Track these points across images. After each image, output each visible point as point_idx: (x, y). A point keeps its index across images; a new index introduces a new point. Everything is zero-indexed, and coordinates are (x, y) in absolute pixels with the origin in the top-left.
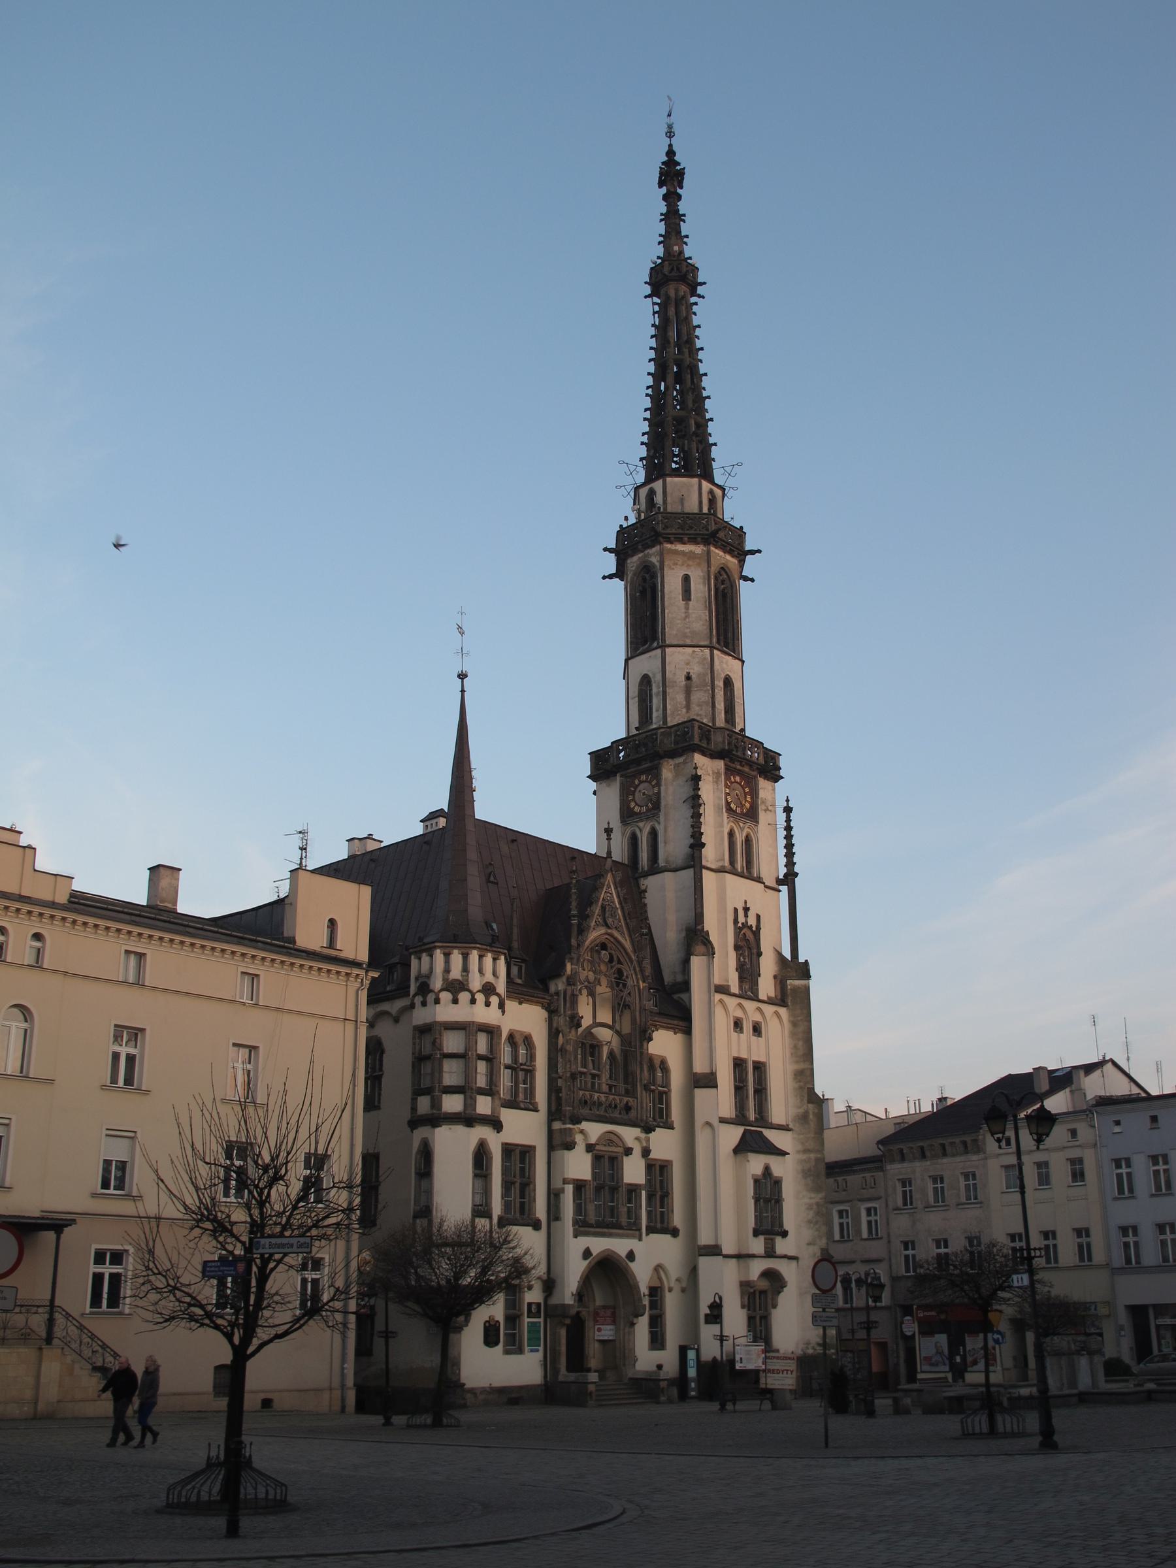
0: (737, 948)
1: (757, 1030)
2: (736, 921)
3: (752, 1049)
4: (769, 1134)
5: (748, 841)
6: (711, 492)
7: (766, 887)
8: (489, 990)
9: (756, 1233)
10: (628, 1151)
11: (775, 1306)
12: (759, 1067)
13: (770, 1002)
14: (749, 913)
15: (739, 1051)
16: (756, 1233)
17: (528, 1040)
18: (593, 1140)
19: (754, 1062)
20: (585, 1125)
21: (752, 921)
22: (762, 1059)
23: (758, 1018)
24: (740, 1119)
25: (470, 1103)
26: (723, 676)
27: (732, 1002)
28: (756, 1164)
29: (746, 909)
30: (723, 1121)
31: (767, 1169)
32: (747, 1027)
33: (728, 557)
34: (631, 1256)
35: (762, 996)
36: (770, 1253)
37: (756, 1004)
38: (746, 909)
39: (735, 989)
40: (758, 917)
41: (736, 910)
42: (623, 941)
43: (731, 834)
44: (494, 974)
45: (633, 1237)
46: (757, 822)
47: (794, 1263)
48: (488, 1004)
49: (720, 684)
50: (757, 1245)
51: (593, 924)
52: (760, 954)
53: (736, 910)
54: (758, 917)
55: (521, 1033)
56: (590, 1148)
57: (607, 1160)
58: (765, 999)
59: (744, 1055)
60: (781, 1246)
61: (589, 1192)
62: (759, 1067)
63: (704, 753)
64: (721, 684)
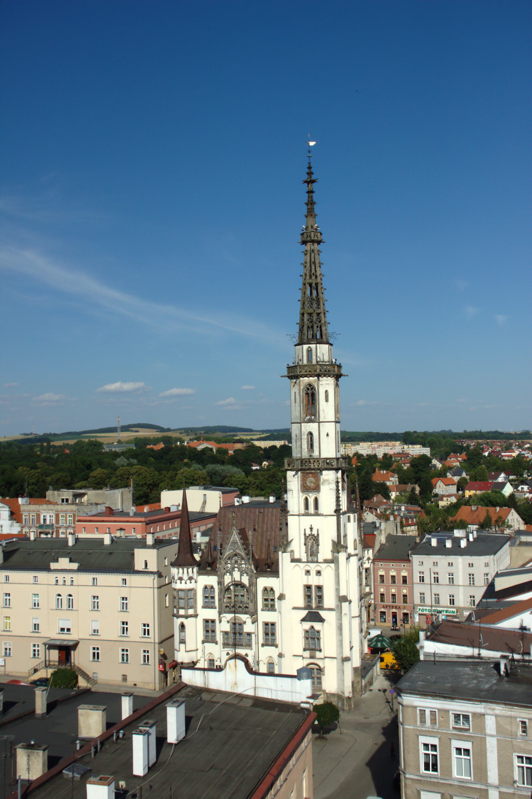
0: (305, 544)
1: (319, 573)
2: (305, 534)
3: (314, 581)
4: (323, 613)
5: (316, 500)
6: (309, 347)
7: (326, 515)
8: (181, 579)
9: (305, 650)
10: (245, 623)
11: (324, 675)
12: (319, 588)
13: (326, 561)
14: (313, 530)
15: (308, 582)
16: (305, 650)
17: (212, 587)
18: (228, 619)
19: (315, 586)
20: (224, 615)
21: (315, 532)
22: (321, 584)
23: (318, 568)
24: (308, 607)
25: (178, 611)
26: (307, 433)
27: (301, 565)
28: (307, 625)
29: (311, 529)
30: (295, 608)
31: (312, 627)
32: (313, 573)
33: (311, 378)
34: (247, 655)
35: (319, 561)
36: (312, 657)
37: (316, 564)
38: (311, 529)
39: (304, 559)
40: (318, 530)
41: (305, 530)
42: (241, 553)
43: (306, 499)
44: (183, 573)
45: (248, 649)
46: (320, 491)
47: (335, 660)
48: (181, 583)
49: (305, 437)
50: (307, 654)
51: (228, 549)
52: (318, 545)
53: (305, 530)
54: (318, 530)
55: (209, 585)
56: (228, 622)
57: (236, 625)
58: (322, 561)
59: (310, 583)
60: (318, 654)
61: (231, 635)
62: (319, 588)
63: (291, 470)
64: (306, 437)
